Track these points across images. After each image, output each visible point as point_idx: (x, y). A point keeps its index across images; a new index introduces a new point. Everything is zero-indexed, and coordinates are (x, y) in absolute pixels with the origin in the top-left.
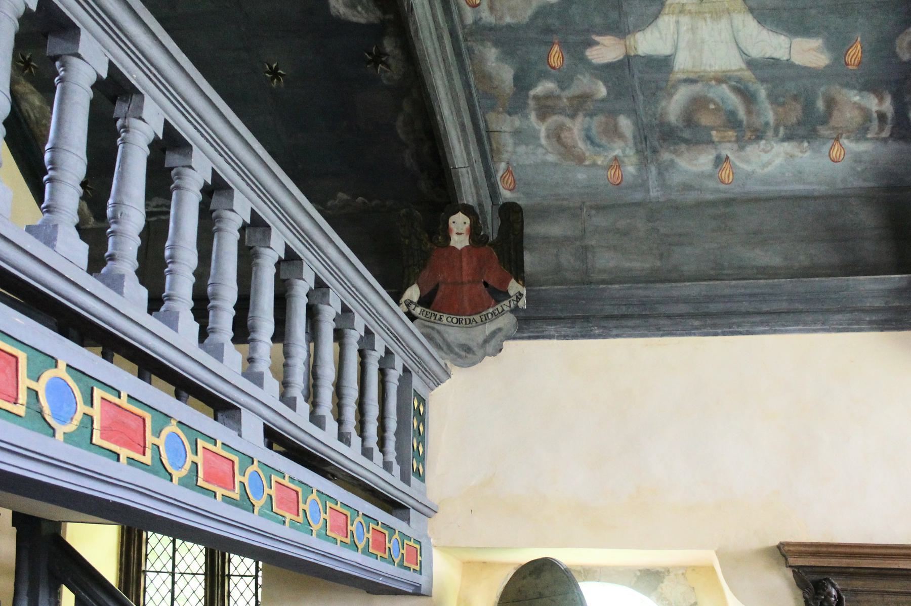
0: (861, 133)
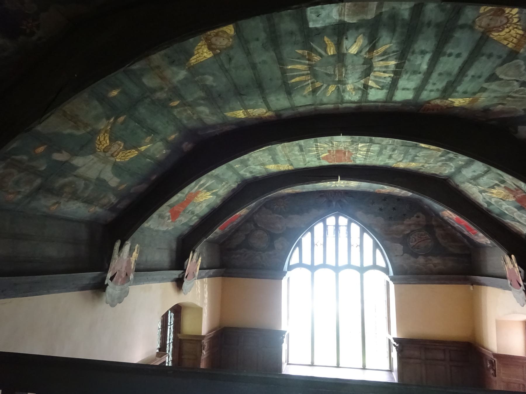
0: (102, 206)
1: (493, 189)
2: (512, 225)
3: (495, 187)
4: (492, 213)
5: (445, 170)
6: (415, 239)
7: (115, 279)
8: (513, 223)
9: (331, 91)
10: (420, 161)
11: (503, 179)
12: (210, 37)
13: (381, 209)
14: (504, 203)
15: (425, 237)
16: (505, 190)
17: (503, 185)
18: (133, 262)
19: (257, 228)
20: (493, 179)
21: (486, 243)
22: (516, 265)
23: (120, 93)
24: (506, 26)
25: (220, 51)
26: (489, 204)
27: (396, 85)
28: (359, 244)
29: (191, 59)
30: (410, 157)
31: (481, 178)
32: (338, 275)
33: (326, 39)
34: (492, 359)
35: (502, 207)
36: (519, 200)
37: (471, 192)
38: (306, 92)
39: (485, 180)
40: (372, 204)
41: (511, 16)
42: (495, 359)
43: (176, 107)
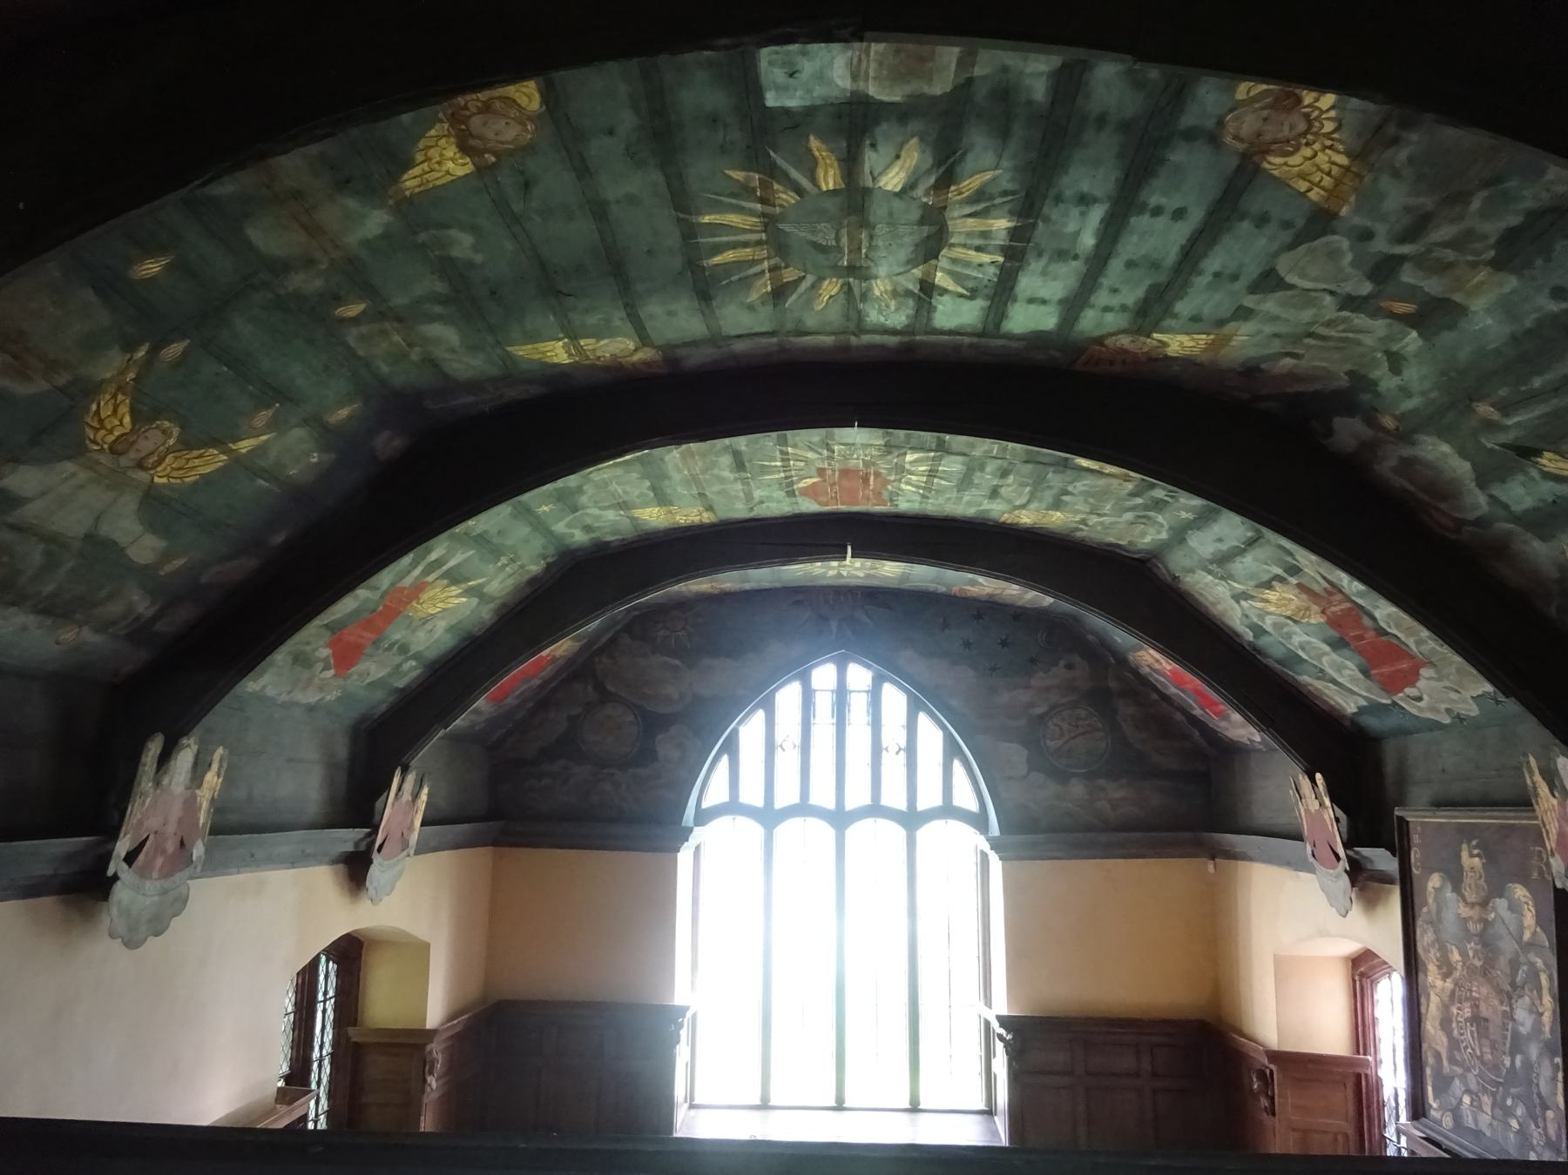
0: (102, 627)
1: (1268, 589)
2: (1317, 689)
3: (1274, 583)
4: (1266, 656)
5: (1144, 534)
6: (1061, 729)
7: (141, 857)
8: (1319, 684)
9: (828, 297)
10: (1077, 507)
11: (1295, 562)
12: (467, 113)
13: (967, 644)
14: (1296, 628)
15: (1088, 725)
16: (1299, 593)
17: (1294, 581)
18: (205, 805)
19: (605, 696)
20: (1269, 562)
21: (1249, 739)
22: (1327, 802)
23: (167, 268)
26: (1259, 631)
27: (1012, 288)
28: (903, 744)
29: (406, 177)
30: (1048, 496)
31: (1238, 559)
32: (844, 835)
33: (814, 143)
34: (1263, 1065)
35: (1293, 640)
36: (1334, 622)
37: (1211, 599)
38: (753, 297)
39: (1247, 563)
40: (943, 630)
41: (1316, 113)
42: (1272, 1067)
43: (355, 321)
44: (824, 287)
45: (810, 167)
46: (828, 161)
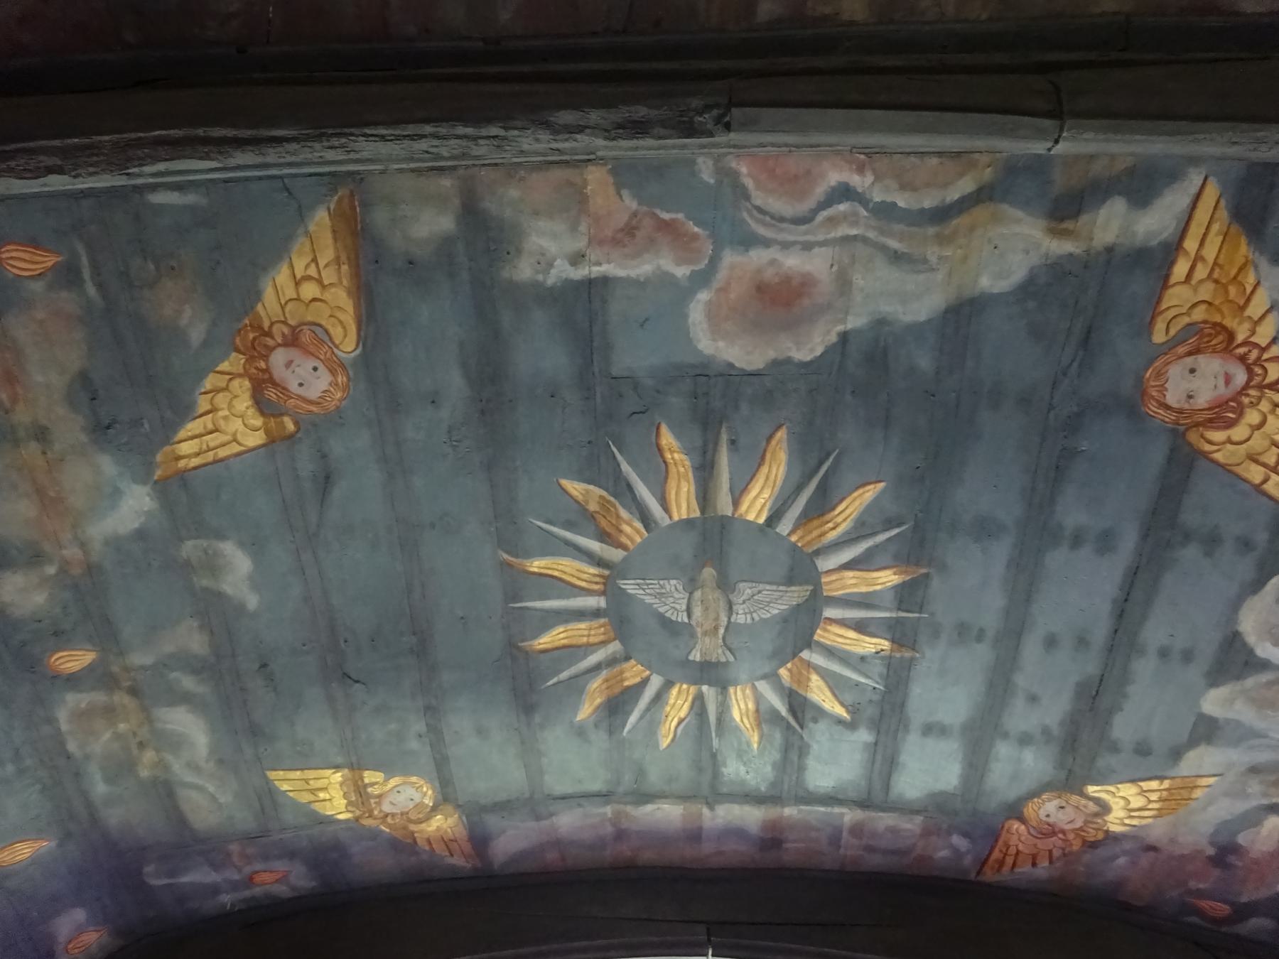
9: (676, 720)
12: (270, 342)
24: (1246, 400)
25: (296, 423)
27: (903, 705)
29: (182, 434)
33: (668, 439)
38: (585, 711)
41: (1254, 354)
43: (73, 681)
44: (672, 701)
45: (660, 481)
46: (682, 470)
